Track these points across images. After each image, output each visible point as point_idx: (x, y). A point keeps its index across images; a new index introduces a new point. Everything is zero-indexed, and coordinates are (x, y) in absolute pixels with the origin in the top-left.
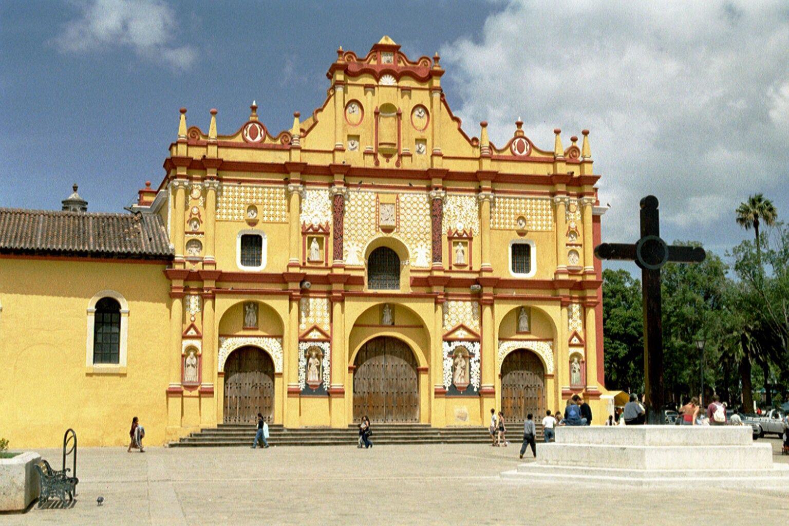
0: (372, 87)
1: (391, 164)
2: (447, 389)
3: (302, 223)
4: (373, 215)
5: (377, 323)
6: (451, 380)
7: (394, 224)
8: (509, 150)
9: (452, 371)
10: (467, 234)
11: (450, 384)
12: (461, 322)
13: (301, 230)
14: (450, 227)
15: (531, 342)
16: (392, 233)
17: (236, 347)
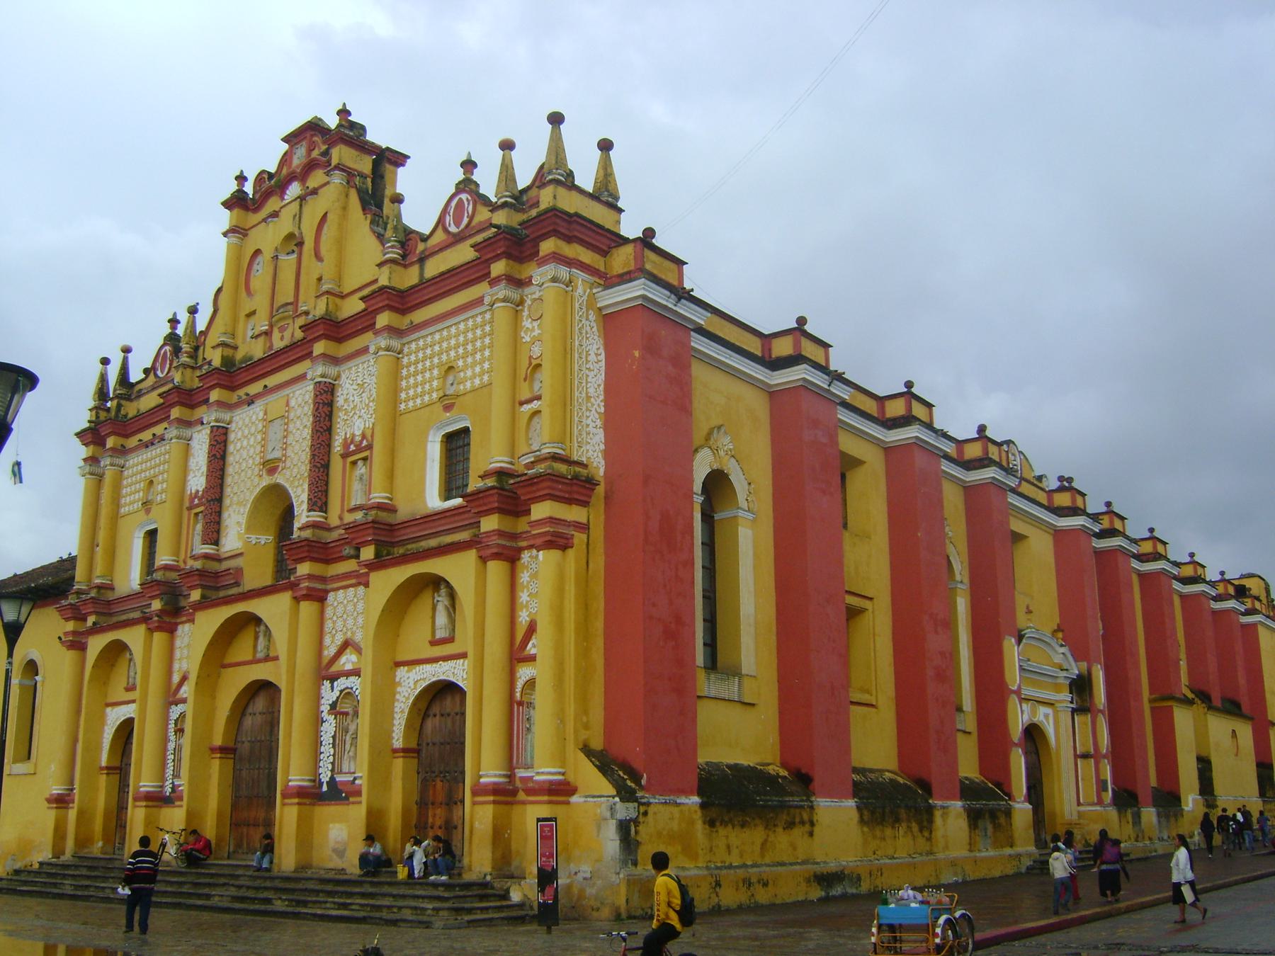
0: (275, 214)
1: (286, 342)
2: (325, 788)
3: (189, 492)
4: (259, 448)
5: (250, 658)
6: (330, 767)
7: (277, 454)
8: (440, 231)
9: (334, 747)
10: (367, 441)
11: (329, 774)
12: (349, 634)
13: (187, 504)
14: (346, 434)
15: (451, 663)
16: (276, 475)
17: (118, 723)
